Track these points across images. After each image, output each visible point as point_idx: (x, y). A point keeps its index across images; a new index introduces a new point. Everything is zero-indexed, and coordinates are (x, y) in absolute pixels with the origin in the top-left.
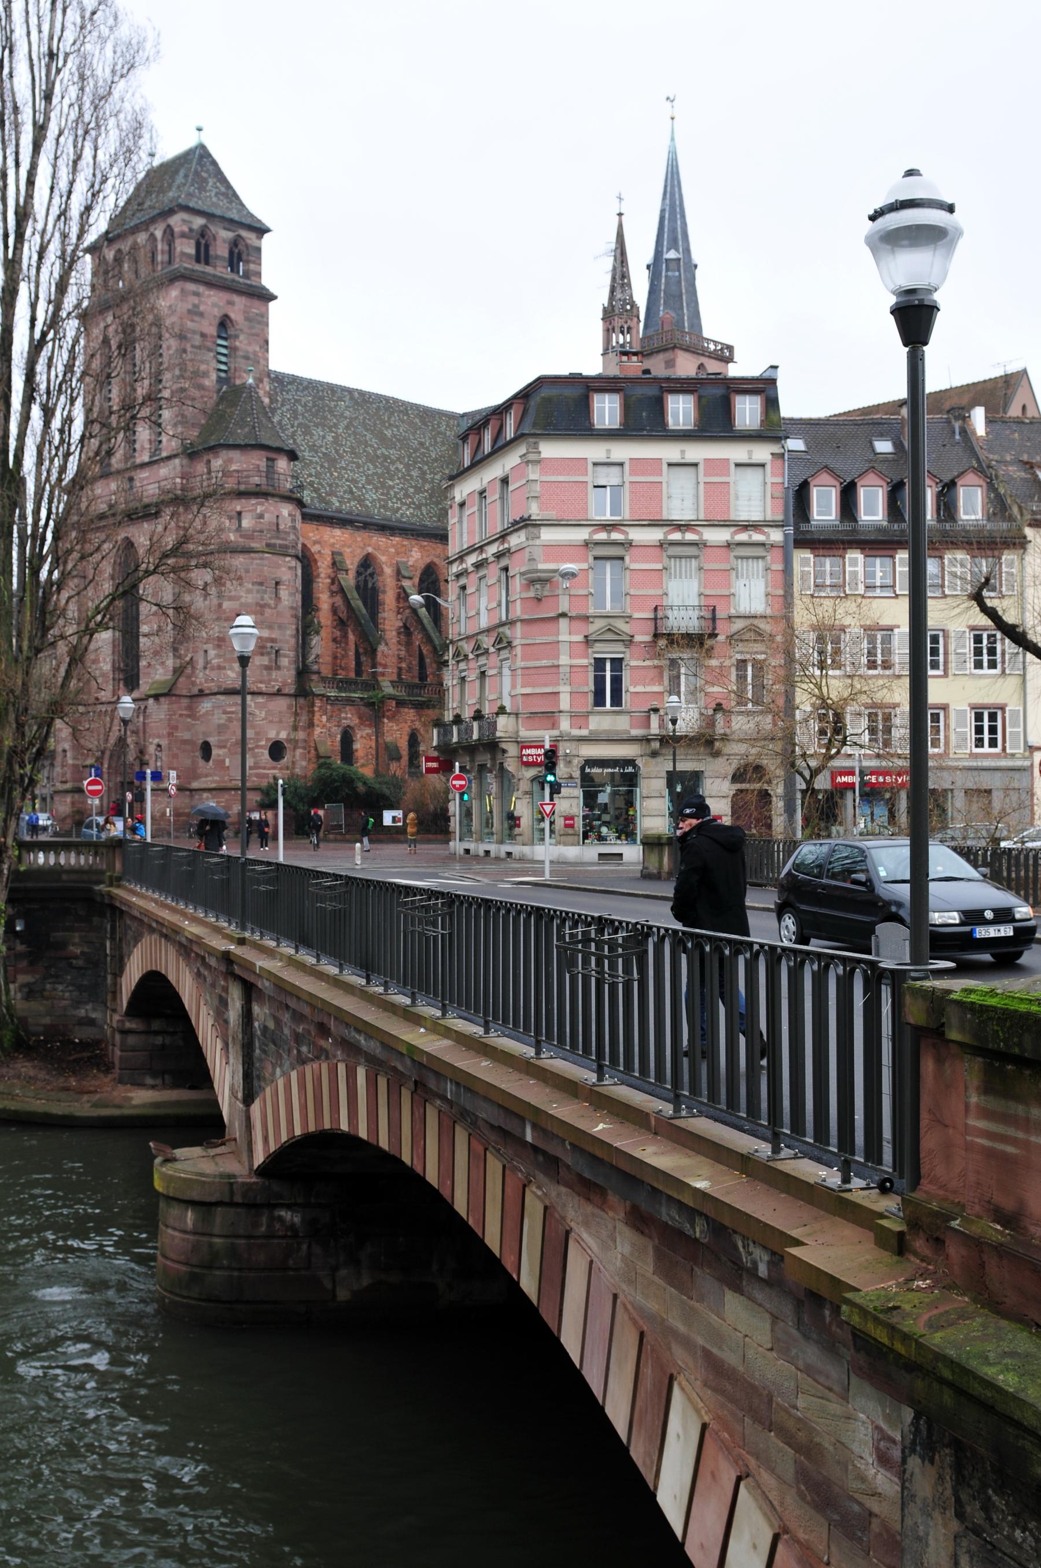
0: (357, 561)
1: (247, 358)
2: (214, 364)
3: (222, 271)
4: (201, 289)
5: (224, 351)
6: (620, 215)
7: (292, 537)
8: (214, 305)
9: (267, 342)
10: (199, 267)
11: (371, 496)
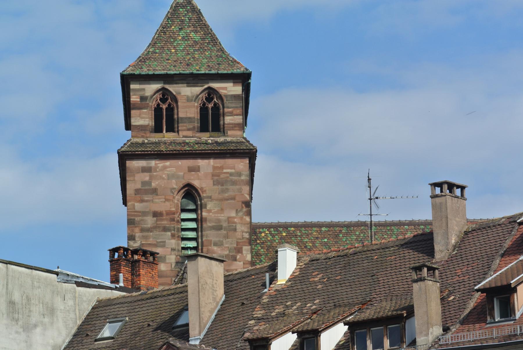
1: (219, 228)
2: (173, 243)
3: (187, 135)
4: (153, 163)
5: (193, 225)
8: (170, 177)
10: (155, 138)
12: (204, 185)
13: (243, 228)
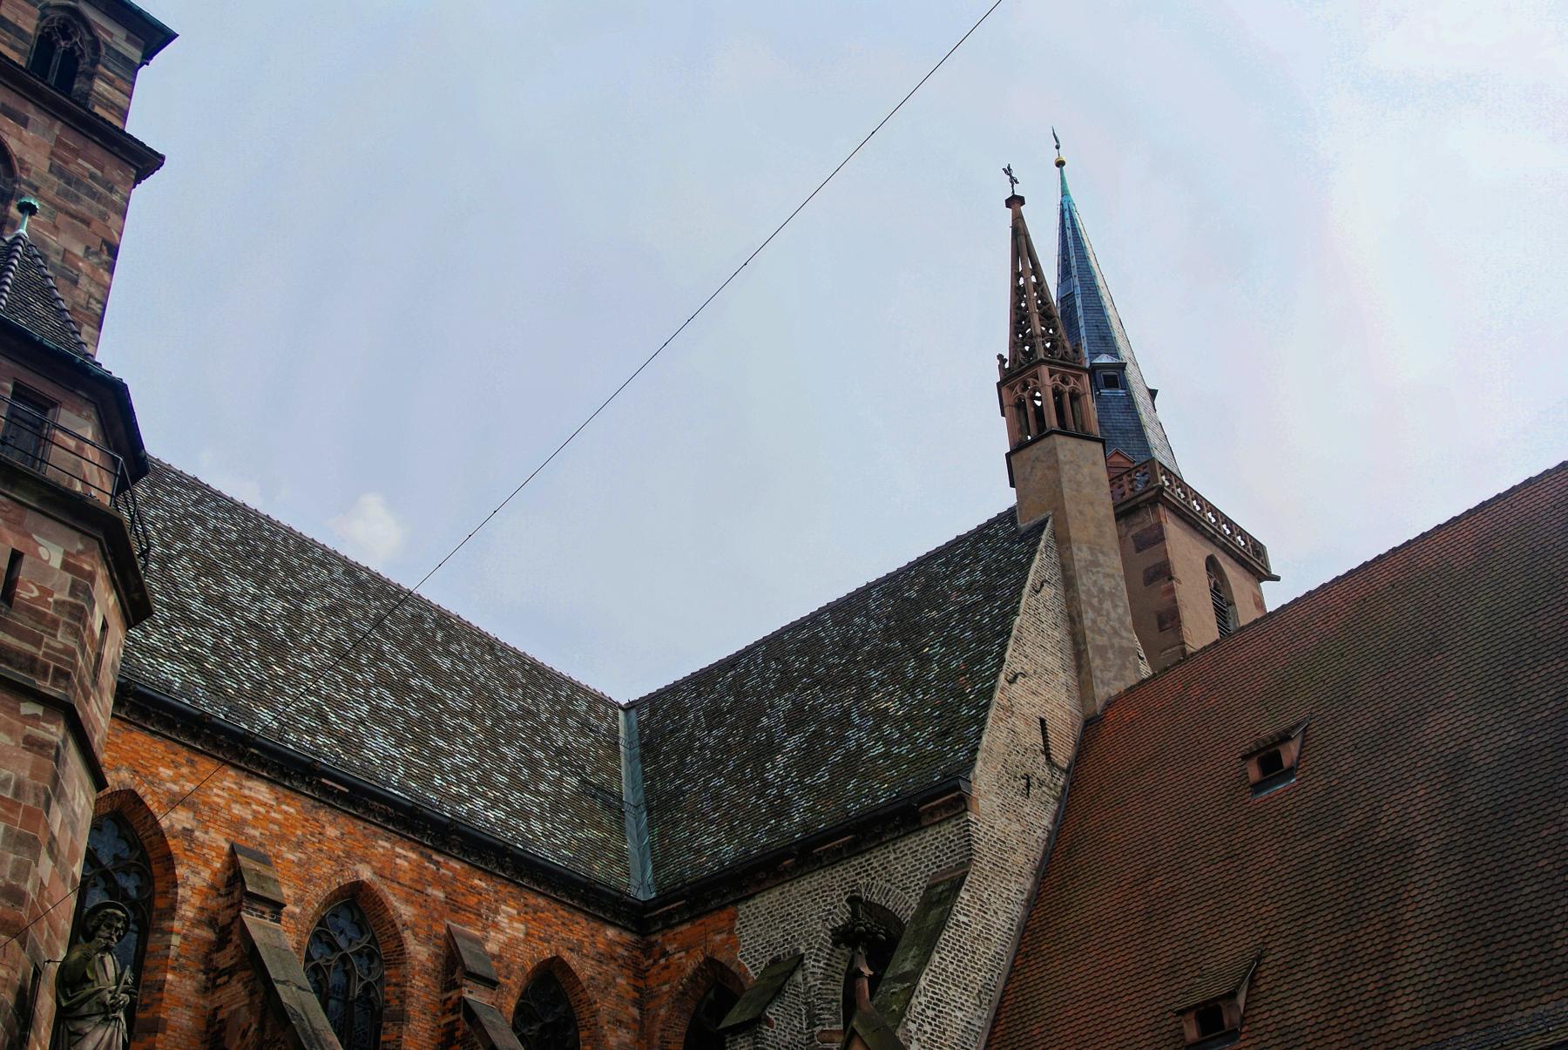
0: (317, 894)
6: (1015, 202)
7: (62, 639)
9: (113, 251)
11: (378, 744)
12: (28, 158)
13: (92, 290)
